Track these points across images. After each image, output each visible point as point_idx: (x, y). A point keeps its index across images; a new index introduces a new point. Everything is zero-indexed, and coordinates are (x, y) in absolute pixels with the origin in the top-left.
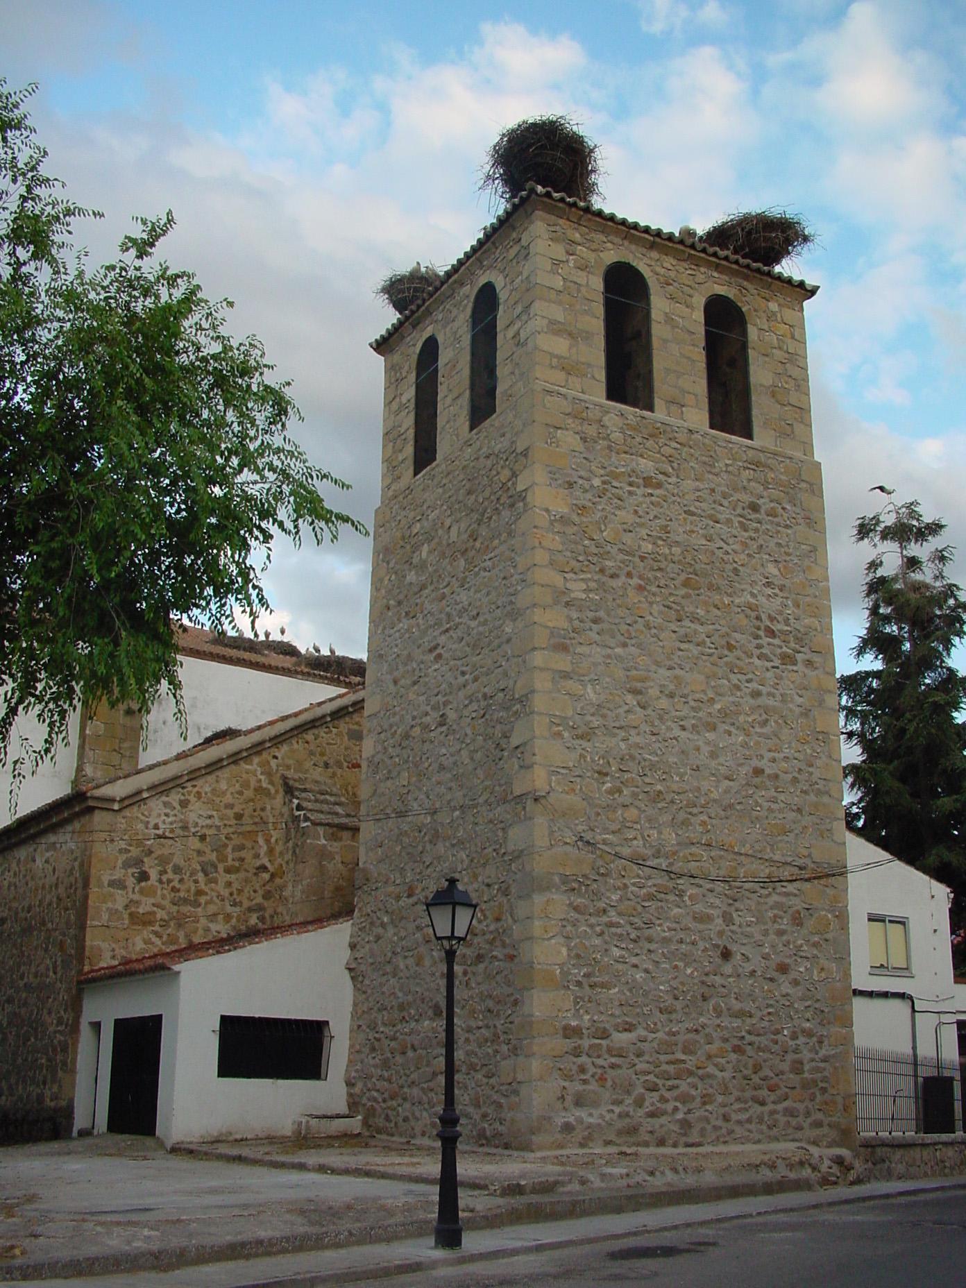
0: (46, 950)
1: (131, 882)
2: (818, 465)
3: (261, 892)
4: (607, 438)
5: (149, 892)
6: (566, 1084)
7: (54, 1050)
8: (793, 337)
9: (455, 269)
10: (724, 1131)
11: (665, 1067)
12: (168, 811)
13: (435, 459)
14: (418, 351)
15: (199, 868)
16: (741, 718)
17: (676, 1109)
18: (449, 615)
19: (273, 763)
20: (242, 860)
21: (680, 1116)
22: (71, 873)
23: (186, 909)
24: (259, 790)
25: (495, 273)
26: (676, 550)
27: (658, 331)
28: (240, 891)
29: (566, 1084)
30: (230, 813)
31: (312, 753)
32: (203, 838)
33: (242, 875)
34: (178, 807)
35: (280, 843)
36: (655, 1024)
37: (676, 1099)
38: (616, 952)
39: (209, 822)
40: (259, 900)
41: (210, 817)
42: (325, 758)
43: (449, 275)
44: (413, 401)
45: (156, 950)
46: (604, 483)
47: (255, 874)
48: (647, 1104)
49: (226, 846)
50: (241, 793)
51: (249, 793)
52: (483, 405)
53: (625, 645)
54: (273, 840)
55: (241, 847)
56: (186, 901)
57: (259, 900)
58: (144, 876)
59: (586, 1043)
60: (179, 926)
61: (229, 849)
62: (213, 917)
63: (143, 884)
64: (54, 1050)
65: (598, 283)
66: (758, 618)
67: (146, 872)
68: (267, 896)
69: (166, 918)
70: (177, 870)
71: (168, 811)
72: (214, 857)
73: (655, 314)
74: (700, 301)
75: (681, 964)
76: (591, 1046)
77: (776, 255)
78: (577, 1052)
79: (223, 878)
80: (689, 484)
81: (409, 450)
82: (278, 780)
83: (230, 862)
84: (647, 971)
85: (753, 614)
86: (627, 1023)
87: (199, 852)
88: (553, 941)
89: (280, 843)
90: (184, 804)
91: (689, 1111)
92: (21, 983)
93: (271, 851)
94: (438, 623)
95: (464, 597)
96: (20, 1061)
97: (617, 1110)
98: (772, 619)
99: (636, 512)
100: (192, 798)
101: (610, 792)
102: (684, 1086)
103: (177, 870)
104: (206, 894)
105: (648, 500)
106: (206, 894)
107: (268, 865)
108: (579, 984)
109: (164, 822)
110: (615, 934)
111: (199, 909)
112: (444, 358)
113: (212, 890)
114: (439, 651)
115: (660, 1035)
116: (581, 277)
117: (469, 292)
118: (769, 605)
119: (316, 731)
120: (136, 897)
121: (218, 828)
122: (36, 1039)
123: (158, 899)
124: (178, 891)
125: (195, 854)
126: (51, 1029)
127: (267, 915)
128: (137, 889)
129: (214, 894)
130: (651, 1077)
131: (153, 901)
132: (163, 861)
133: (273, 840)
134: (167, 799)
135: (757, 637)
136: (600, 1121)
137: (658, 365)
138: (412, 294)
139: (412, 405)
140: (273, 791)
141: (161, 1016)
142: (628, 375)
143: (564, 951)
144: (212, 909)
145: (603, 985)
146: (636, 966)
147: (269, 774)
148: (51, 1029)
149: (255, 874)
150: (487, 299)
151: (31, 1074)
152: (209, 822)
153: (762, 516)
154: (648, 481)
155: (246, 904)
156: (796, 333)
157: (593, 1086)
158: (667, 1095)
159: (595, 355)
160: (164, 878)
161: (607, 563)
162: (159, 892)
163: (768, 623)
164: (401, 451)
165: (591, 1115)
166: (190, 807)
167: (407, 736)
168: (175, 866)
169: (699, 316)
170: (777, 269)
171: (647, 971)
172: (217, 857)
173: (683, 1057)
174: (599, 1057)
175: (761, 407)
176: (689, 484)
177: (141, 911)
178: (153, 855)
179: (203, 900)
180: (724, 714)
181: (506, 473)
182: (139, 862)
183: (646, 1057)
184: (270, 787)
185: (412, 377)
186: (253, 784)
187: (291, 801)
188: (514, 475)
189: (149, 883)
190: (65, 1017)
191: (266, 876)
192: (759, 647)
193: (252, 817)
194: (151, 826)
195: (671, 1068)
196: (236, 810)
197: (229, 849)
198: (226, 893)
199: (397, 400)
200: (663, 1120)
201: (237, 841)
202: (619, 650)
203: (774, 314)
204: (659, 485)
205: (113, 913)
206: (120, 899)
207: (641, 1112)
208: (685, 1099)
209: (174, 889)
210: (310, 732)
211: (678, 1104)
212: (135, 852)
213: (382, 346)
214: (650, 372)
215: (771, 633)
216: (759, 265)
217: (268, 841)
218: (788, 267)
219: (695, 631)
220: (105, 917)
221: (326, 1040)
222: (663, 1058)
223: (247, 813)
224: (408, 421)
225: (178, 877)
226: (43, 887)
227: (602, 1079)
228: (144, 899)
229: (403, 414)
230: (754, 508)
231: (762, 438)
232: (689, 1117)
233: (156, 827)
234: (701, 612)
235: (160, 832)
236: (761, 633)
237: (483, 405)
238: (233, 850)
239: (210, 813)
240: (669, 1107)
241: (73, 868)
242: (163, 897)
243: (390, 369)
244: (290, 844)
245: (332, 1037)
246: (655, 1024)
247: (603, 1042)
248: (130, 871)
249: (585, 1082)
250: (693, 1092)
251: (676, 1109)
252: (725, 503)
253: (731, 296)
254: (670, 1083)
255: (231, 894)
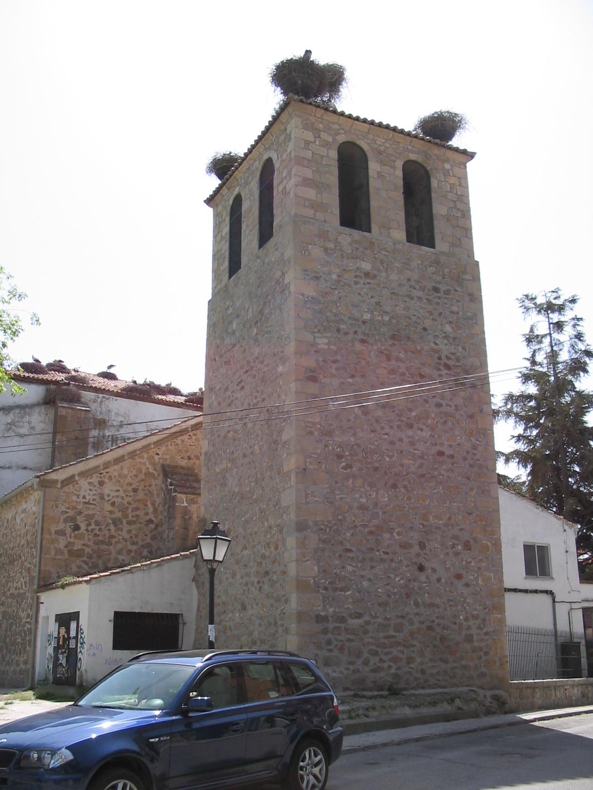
0: (21, 573)
1: (69, 531)
2: (477, 264)
3: (150, 536)
4: (341, 250)
5: (81, 537)
6: (318, 652)
7: (25, 633)
8: (460, 185)
9: (250, 151)
10: (422, 681)
11: (382, 641)
12: (91, 488)
13: (240, 268)
14: (231, 204)
15: (111, 522)
16: (429, 421)
17: (390, 667)
18: (248, 362)
19: (156, 457)
20: (138, 516)
21: (393, 671)
22: (34, 526)
23: (103, 547)
24: (148, 474)
25: (272, 151)
26: (386, 318)
27: (374, 184)
28: (136, 536)
29: (318, 652)
30: (130, 488)
31: (180, 451)
32: (113, 504)
33: (137, 526)
34: (98, 485)
35: (161, 505)
36: (376, 614)
37: (390, 660)
38: (350, 568)
39: (117, 494)
40: (148, 540)
41: (118, 491)
42: (188, 454)
43: (246, 155)
44: (228, 234)
45: (85, 572)
46: (339, 276)
47: (146, 525)
48: (371, 664)
49: (128, 508)
50: (136, 476)
51: (142, 476)
52: (266, 234)
53: (353, 376)
54: (157, 504)
55: (137, 509)
56: (103, 542)
57: (148, 540)
58: (77, 528)
59: (331, 626)
60: (99, 557)
61: (130, 510)
62: (120, 552)
63: (76, 532)
64: (25, 633)
65: (334, 154)
66: (440, 358)
67: (78, 525)
68: (153, 538)
69: (91, 552)
70: (97, 523)
71: (91, 488)
72: (120, 515)
73: (371, 173)
74: (399, 164)
75: (392, 576)
76: (335, 628)
77: (450, 136)
78: (325, 631)
79: (126, 527)
80: (393, 277)
81: (226, 263)
82: (159, 468)
83: (130, 518)
84: (370, 580)
85: (436, 355)
86: (358, 613)
87: (111, 512)
88: (309, 562)
89: (161, 505)
90: (101, 483)
91: (399, 668)
92: (9, 593)
93: (155, 510)
94: (242, 367)
95: (256, 351)
96: (8, 640)
97: (351, 668)
98: (448, 358)
99: (359, 294)
100: (106, 480)
101: (344, 468)
102: (395, 651)
103: (97, 523)
104: (116, 537)
105: (367, 286)
106: (116, 537)
107: (154, 519)
108: (326, 589)
109: (89, 495)
110: (349, 557)
111: (111, 547)
112: (245, 207)
113: (119, 535)
114: (243, 384)
115: (379, 620)
116: (323, 151)
117: (258, 166)
118: (445, 349)
119: (182, 437)
120: (72, 540)
121: (123, 498)
122: (16, 626)
123: (86, 541)
124: (98, 536)
125: (108, 513)
126: (24, 621)
127: (153, 550)
128: (72, 535)
129: (121, 538)
130: (374, 647)
131: (82, 542)
132: (89, 517)
133: (157, 504)
134: (90, 481)
135: (439, 370)
136: (341, 675)
137: (374, 203)
138: (223, 167)
139: (228, 237)
140: (156, 475)
141: (79, 612)
142: (354, 211)
143: (316, 568)
144: (119, 546)
145: (341, 590)
146: (362, 576)
147: (154, 464)
148: (24, 621)
149: (146, 525)
150: (268, 169)
151: (13, 648)
152: (117, 494)
153: (441, 294)
154: (367, 275)
155: (140, 543)
156: (462, 181)
157: (336, 653)
158: (385, 658)
159: (332, 198)
160: (90, 528)
161: (342, 326)
162: (86, 536)
163: (446, 361)
164: (222, 265)
165: (334, 671)
166: (105, 485)
167: (225, 437)
168: (96, 521)
169: (399, 173)
170: (450, 143)
171: (370, 580)
172: (122, 515)
173: (394, 634)
174: (339, 634)
175: (441, 229)
176: (393, 277)
177: (75, 548)
178: (83, 515)
179: (114, 541)
180: (419, 418)
181: (279, 273)
182: (73, 519)
183: (370, 635)
184: (154, 472)
185: (228, 219)
186: (144, 470)
187: (167, 481)
188: (283, 274)
189: (80, 531)
190: (31, 613)
191: (152, 526)
192: (440, 376)
193: (143, 490)
194: (81, 497)
195: (386, 641)
196: (133, 486)
197: (130, 510)
198: (127, 536)
199: (220, 233)
200: (382, 674)
201: (134, 505)
202: (350, 380)
203: (448, 171)
204: (375, 277)
205: (59, 551)
206: (62, 543)
207: (367, 669)
208: (395, 660)
209: (96, 535)
210: (179, 438)
211: (391, 664)
212: (71, 513)
213: (209, 201)
214: (369, 209)
215: (448, 367)
216: (438, 141)
217: (153, 504)
218: (455, 142)
219: (399, 367)
220: (53, 552)
221: (181, 626)
222: (381, 635)
223: (141, 488)
224: (226, 246)
225: (97, 528)
226: (20, 535)
227: (341, 649)
228: (77, 541)
229: (223, 242)
230: (436, 290)
231: (441, 245)
232: (399, 672)
233: (84, 497)
234: (402, 355)
235: (87, 501)
236: (441, 367)
237: (266, 234)
238: (132, 511)
239: (117, 489)
240: (385, 665)
241: (35, 524)
242: (89, 540)
243: (216, 216)
244: (166, 506)
245: (184, 624)
246: (376, 614)
247: (343, 625)
248: (69, 524)
249: (330, 650)
250: (401, 656)
251: (390, 667)
252: (417, 287)
253: (420, 160)
254: (385, 650)
255: (131, 537)
